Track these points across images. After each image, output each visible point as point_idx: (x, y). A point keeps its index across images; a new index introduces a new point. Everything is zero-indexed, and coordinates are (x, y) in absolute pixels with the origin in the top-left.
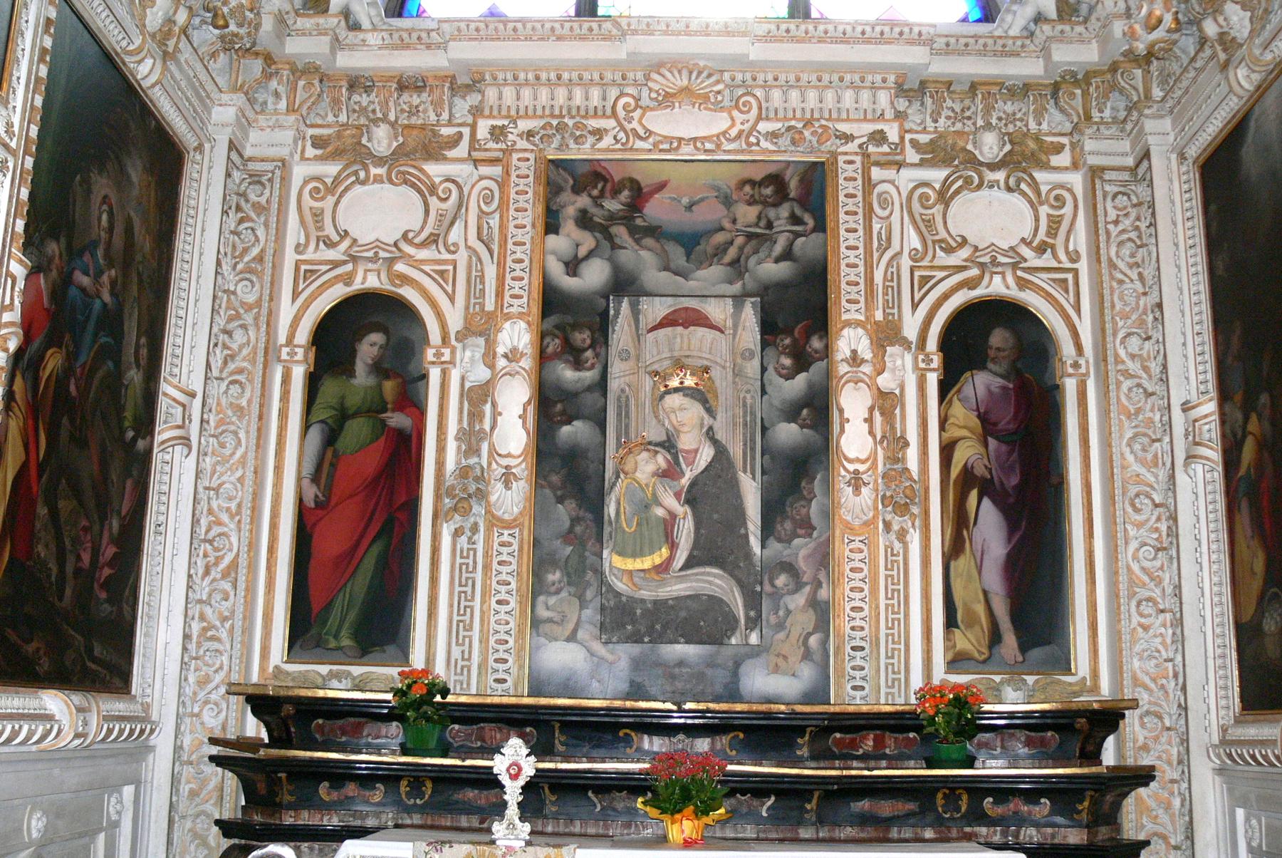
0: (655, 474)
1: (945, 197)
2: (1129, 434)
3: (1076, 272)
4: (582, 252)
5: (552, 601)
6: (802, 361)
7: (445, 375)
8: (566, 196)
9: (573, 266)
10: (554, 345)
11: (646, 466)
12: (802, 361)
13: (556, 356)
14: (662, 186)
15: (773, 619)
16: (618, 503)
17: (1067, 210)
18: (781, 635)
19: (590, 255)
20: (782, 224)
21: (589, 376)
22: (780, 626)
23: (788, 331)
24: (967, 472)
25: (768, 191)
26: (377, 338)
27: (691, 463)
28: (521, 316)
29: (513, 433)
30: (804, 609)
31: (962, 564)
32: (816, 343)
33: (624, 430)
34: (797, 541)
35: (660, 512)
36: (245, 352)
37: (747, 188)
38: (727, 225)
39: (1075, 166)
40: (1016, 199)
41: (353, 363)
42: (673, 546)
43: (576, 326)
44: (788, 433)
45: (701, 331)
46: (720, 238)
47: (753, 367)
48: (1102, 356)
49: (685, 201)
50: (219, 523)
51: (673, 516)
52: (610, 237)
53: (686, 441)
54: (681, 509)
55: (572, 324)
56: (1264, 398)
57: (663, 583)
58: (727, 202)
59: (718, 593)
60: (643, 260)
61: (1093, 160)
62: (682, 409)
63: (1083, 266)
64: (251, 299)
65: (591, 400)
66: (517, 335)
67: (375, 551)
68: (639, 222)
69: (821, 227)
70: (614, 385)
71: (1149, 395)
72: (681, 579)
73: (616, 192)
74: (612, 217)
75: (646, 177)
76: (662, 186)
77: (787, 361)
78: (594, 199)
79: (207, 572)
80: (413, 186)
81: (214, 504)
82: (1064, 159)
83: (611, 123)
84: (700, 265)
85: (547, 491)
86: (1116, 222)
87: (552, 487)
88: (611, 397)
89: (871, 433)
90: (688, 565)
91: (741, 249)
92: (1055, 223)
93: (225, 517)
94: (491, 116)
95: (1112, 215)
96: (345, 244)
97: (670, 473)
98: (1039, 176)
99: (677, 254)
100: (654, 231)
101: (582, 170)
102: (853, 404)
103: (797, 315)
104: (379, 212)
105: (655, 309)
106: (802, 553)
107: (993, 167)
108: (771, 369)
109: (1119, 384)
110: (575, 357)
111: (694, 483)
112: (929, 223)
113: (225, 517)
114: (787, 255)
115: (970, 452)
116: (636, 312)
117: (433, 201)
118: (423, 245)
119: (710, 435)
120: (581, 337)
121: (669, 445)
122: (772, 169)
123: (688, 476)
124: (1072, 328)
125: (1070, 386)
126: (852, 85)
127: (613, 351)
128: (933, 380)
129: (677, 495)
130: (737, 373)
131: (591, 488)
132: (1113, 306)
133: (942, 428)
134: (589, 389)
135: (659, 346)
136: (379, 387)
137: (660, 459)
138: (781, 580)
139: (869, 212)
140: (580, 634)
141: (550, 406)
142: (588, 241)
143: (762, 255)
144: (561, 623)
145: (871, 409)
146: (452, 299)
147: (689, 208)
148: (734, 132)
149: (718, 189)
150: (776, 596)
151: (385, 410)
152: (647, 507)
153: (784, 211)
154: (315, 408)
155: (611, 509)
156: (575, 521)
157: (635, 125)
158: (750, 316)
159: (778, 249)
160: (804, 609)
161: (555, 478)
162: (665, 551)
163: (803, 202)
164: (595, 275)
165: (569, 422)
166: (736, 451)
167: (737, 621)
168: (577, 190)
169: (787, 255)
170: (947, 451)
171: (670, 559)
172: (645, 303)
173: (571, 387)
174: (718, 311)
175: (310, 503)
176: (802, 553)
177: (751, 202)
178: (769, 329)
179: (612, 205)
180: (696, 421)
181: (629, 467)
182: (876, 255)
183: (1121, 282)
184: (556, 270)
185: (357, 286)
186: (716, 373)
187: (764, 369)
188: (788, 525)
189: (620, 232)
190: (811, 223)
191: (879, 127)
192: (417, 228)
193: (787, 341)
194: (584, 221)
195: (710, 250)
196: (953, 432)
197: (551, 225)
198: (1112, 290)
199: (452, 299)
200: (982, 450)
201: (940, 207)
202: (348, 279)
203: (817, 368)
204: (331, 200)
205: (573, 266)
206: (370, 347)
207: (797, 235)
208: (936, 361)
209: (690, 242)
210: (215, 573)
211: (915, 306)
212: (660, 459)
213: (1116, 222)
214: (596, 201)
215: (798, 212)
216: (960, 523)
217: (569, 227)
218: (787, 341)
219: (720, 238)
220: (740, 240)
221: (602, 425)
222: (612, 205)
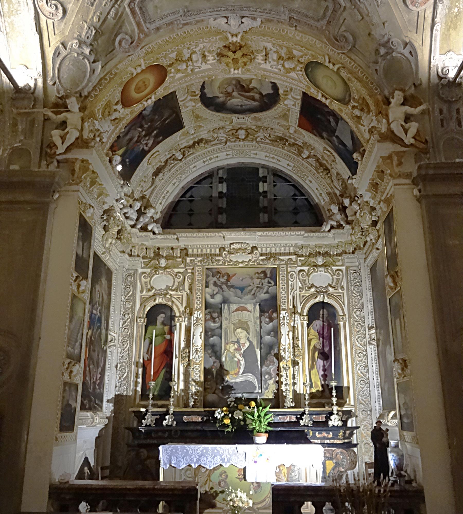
0: (235, 350)
1: (308, 275)
2: (357, 337)
3: (343, 293)
4: (215, 293)
5: (209, 383)
6: (271, 320)
7: (180, 325)
8: (211, 278)
9: (212, 296)
10: (208, 317)
11: (232, 348)
12: (271, 320)
13: (209, 320)
14: (235, 275)
15: (265, 387)
16: (226, 357)
17: (341, 277)
18: (267, 391)
19: (217, 293)
20: (266, 284)
21: (217, 325)
22: (267, 388)
23: (268, 312)
24: (315, 347)
25: (262, 275)
26: (163, 315)
27: (243, 347)
28: (200, 309)
29: (198, 341)
30: (273, 384)
31: (314, 371)
32: (275, 315)
33: (226, 339)
34: (271, 366)
35: (236, 359)
36: (129, 320)
37: (257, 275)
38: (251, 284)
39: (342, 265)
40: (327, 274)
41: (156, 322)
42: (239, 368)
43: (214, 312)
44: (268, 338)
45: (245, 312)
46: (250, 288)
47: (258, 321)
48: (349, 317)
49: (241, 278)
50: (123, 366)
51: (239, 360)
52: (222, 289)
53: (242, 341)
54: (241, 359)
55: (213, 311)
56: (382, 331)
57: (237, 378)
58: (252, 278)
59: (251, 380)
60: (230, 294)
61: (347, 264)
62: (241, 333)
63: (345, 292)
64: (130, 306)
65: (217, 331)
66: (198, 315)
67: (164, 371)
68: (229, 284)
69: (276, 284)
70: (223, 327)
71: (362, 326)
72: (242, 377)
73: (223, 277)
74: (222, 283)
75: (231, 272)
76: (235, 275)
77: (267, 320)
78: (218, 278)
79: (120, 378)
80: (171, 275)
81: (121, 361)
82: (340, 263)
83: (221, 258)
84: (245, 295)
85: (207, 355)
86: (354, 280)
87: (209, 354)
88: (223, 330)
89: (288, 338)
90: (242, 374)
91: (255, 291)
92: (338, 280)
93: (124, 364)
94: (191, 257)
95: (352, 278)
96: (154, 291)
97: (239, 349)
98: (333, 267)
99: (239, 292)
100: (232, 287)
101: (214, 271)
102: (284, 330)
103: (270, 307)
104: (162, 281)
105: (234, 307)
106: (272, 369)
107: (321, 266)
108: (263, 322)
109: (354, 324)
110: (213, 319)
111: (244, 351)
112: (304, 281)
113: (124, 364)
114: (267, 292)
115: (316, 342)
116: (229, 307)
117: (176, 279)
118: (174, 290)
119: (248, 339)
120: (215, 315)
121: (238, 342)
122: (263, 270)
123: (243, 350)
124: (342, 309)
125: (342, 323)
126: (284, 246)
127: (223, 318)
128: (305, 323)
129: (240, 355)
130: (255, 323)
131: (218, 354)
132: (352, 303)
133: (308, 336)
134: (217, 328)
135: (235, 317)
136: (164, 328)
137: (236, 346)
138: (267, 377)
139: (288, 279)
140: (216, 392)
141: (207, 333)
142: (216, 289)
143: (261, 292)
144: (211, 389)
145: (288, 332)
146: (182, 304)
147: (242, 280)
148: (253, 260)
149: (248, 275)
150: (266, 380)
151: (165, 334)
152: (233, 358)
153: (266, 280)
154: (147, 334)
155: (223, 359)
156: (214, 362)
157: (228, 259)
158: (258, 307)
159: (265, 291)
160: (273, 384)
161: (209, 352)
162: (237, 370)
163: (271, 278)
164: (218, 298)
165: (212, 337)
166: (255, 343)
167: (256, 387)
168: (213, 276)
169: (267, 292)
170: (309, 342)
171: (239, 371)
172: (231, 305)
173: (213, 328)
174: (250, 307)
175: (146, 359)
176: (272, 369)
177: (258, 278)
178: (262, 311)
179: (223, 280)
180: (244, 336)
181: (228, 348)
182: (290, 291)
183: (354, 297)
184: (208, 297)
185: (157, 302)
186: (249, 323)
187: (261, 322)
188: (268, 362)
189: (224, 287)
190: (273, 283)
191: (290, 257)
192: (171, 285)
193: (267, 314)
194: (215, 284)
195: (247, 291)
196: (311, 337)
197: (207, 286)
198: (352, 299)
199: (182, 304)
200: (318, 341)
201: (307, 277)
202: (155, 300)
203: (275, 321)
204: (149, 278)
205: (212, 296)
206: (161, 318)
207: (270, 287)
208: (306, 318)
209: (242, 289)
210: (122, 379)
211: (301, 304)
212: (236, 346)
213: (354, 280)
214: (218, 279)
215: (270, 280)
216: (313, 360)
217: (211, 286)
218: (267, 314)
219: (250, 288)
220: (255, 288)
221: (221, 338)
222: (223, 280)
